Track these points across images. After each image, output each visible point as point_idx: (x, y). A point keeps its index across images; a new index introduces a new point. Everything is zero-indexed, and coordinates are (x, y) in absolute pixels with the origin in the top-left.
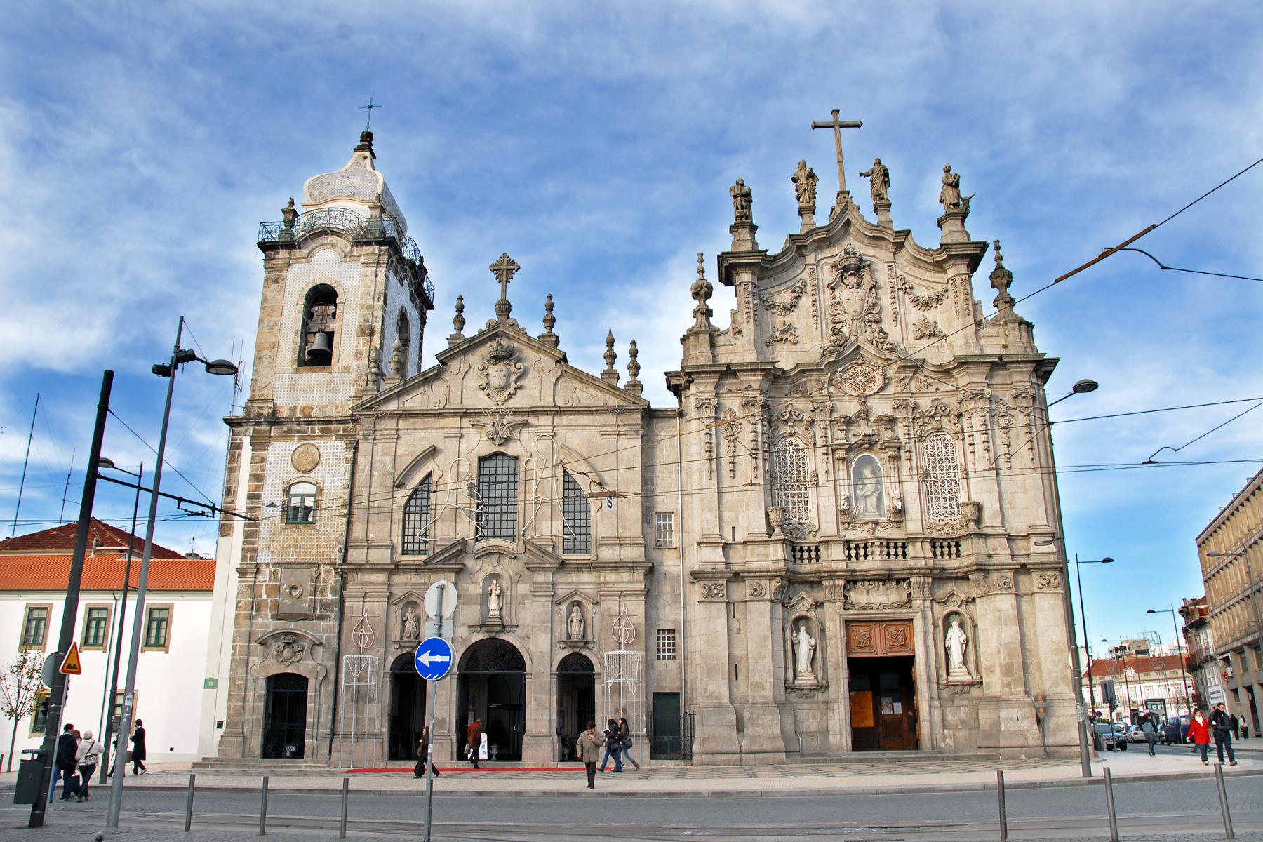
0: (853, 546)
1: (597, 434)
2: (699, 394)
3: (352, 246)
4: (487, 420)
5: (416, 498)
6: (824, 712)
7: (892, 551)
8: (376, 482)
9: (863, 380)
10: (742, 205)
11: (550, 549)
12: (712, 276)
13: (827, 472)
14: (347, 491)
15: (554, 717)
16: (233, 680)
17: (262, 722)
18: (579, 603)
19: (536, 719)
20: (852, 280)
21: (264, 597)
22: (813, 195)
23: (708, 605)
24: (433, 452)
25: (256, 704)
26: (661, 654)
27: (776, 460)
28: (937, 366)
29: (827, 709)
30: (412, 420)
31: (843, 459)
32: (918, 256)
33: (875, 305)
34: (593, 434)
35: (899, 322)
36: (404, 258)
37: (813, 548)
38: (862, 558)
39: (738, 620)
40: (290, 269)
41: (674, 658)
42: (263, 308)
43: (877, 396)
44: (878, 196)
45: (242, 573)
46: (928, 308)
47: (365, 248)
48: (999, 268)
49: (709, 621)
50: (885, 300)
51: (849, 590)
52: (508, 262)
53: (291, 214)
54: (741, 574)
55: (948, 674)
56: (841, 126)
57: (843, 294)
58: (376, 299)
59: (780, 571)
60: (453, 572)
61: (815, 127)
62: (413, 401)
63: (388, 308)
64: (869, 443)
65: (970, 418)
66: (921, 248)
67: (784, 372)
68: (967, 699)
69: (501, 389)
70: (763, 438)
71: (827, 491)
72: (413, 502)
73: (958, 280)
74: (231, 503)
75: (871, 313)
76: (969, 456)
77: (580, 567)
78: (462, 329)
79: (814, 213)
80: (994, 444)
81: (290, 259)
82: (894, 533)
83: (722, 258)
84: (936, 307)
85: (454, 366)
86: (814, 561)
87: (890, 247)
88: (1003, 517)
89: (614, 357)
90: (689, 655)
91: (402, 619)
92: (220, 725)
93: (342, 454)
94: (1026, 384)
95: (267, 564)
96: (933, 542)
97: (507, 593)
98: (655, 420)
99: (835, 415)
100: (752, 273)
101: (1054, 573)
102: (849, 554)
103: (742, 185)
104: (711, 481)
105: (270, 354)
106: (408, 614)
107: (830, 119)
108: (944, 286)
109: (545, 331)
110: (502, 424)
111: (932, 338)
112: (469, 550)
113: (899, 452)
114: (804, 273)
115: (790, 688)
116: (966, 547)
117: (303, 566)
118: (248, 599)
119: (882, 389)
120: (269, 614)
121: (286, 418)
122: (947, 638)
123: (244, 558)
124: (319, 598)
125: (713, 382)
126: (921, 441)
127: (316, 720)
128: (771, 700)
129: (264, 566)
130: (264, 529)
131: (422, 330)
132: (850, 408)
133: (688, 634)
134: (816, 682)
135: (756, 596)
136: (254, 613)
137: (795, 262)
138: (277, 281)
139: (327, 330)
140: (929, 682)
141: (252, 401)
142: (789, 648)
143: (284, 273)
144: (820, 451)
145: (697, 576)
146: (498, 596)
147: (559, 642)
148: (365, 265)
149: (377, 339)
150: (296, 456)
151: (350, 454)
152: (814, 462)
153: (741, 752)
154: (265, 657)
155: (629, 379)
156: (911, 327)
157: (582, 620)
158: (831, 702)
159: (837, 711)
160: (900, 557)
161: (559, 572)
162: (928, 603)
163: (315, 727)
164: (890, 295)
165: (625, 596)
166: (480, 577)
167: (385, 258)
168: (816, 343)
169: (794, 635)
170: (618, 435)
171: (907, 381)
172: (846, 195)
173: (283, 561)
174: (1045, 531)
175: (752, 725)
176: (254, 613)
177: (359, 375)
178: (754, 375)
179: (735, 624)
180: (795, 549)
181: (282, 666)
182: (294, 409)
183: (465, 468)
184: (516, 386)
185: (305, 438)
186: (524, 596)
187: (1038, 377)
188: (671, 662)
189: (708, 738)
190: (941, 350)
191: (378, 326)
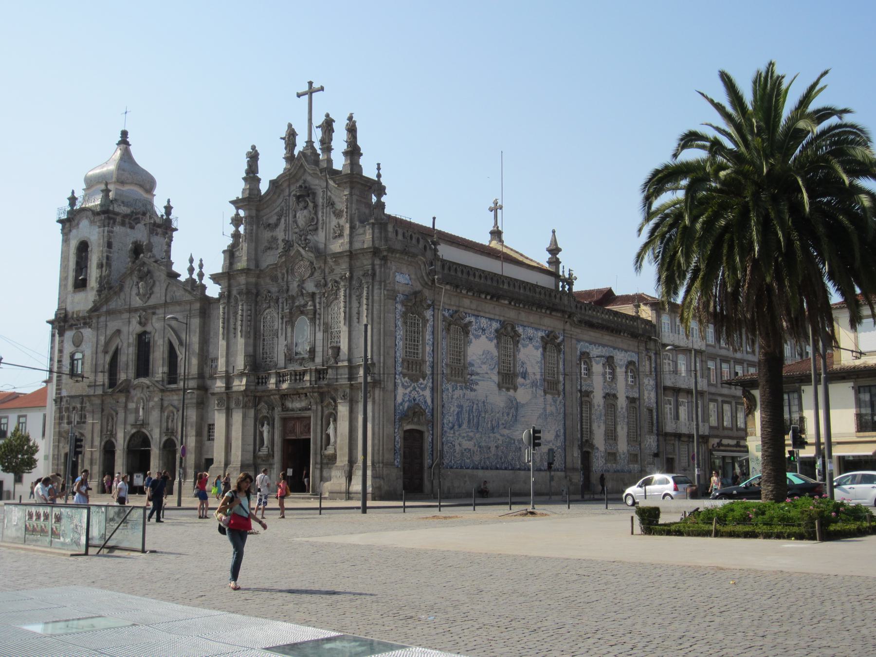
7: (298, 377)
13: (282, 329)
16: (54, 455)
44: (322, 142)
45: (56, 401)
53: (73, 200)
62: (113, 305)
69: (144, 295)
107: (306, 88)
115: (255, 456)
118: (58, 415)
119: (312, 274)
123: (56, 394)
141: (59, 309)
148: (99, 227)
152: (277, 324)
156: (332, 231)
162: (320, 408)
183: (131, 340)
187: (381, 259)
191: (104, 262)
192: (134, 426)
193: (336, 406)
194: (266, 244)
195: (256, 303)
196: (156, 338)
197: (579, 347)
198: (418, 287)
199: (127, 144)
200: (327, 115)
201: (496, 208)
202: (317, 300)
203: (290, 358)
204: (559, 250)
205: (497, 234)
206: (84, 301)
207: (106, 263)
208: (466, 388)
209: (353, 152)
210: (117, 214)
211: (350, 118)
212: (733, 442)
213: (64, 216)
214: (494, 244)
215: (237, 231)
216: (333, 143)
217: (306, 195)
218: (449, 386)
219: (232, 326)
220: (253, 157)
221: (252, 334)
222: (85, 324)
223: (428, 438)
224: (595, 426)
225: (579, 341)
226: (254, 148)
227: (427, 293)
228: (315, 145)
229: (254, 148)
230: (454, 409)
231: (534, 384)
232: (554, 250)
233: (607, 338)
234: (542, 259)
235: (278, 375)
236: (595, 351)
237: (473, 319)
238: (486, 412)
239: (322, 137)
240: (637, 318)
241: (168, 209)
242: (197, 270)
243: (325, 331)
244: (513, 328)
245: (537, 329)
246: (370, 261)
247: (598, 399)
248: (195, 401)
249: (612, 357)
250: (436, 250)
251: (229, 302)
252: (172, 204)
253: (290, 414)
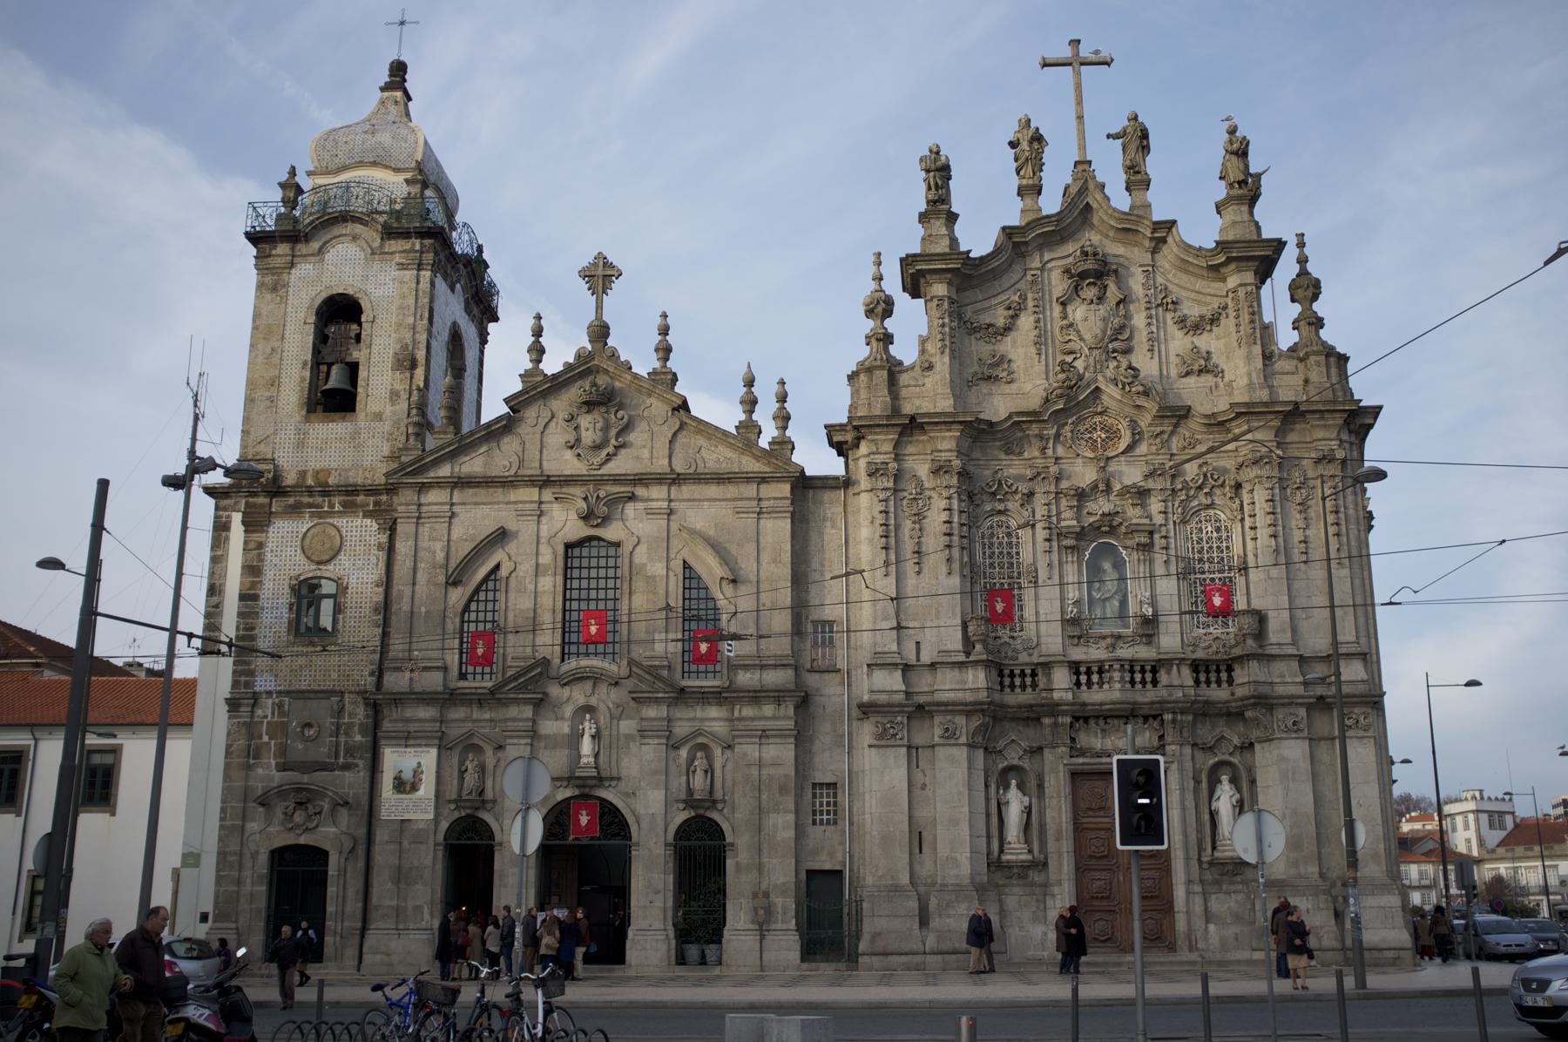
0: (1083, 669)
1: (730, 512)
2: (872, 457)
3: (382, 239)
4: (578, 491)
5: (478, 601)
6: (1041, 898)
7: (1138, 677)
8: (422, 577)
9: (1103, 436)
10: (936, 184)
11: (665, 673)
12: (893, 285)
14: (381, 590)
15: (670, 903)
16: (222, 855)
17: (264, 913)
18: (704, 747)
19: (645, 907)
20: (1090, 293)
21: (266, 738)
22: (1039, 166)
23: (882, 751)
24: (501, 536)
25: (255, 888)
26: (818, 817)
27: (978, 547)
28: (1206, 416)
29: (1045, 895)
30: (471, 491)
31: (1072, 548)
32: (1186, 258)
33: (1122, 327)
34: (723, 512)
35: (1156, 353)
36: (456, 253)
37: (1028, 672)
38: (1096, 686)
39: (923, 771)
40: (293, 271)
41: (835, 823)
42: (255, 328)
43: (1123, 459)
45: (233, 704)
46: (1198, 332)
47: (401, 242)
48: (1303, 273)
49: (882, 773)
50: (1139, 320)
51: (1077, 731)
52: (605, 264)
53: (291, 189)
54: (927, 708)
55: (1214, 848)
56: (1083, 64)
57: (1078, 312)
58: (418, 317)
59: (982, 703)
60: (529, 704)
61: (1045, 65)
62: (473, 464)
63: (434, 330)
65: (1252, 491)
66: (1190, 246)
67: (991, 424)
68: (1241, 883)
69: (597, 447)
70: (960, 517)
71: (1050, 594)
72: (473, 606)
73: (1241, 292)
74: (217, 606)
75: (1117, 339)
76: (1250, 545)
77: (706, 697)
78: (540, 361)
79: (1039, 193)
80: (1284, 528)
81: (293, 256)
82: (1143, 652)
83: (907, 261)
84: (1211, 330)
85: (530, 414)
86: (1029, 690)
87: (1147, 243)
88: (1294, 630)
89: (754, 402)
90: (855, 819)
91: (460, 769)
92: (204, 918)
93: (373, 538)
94: (1334, 443)
95: (269, 693)
96: (1196, 666)
97: (605, 733)
98: (811, 491)
99: (1064, 484)
100: (948, 283)
101: (1363, 710)
102: (1078, 680)
103: (938, 153)
104: (888, 578)
105: (267, 394)
106: (468, 763)
107: (1066, 52)
108: (1222, 300)
109: (657, 365)
110: (598, 496)
111: (1203, 375)
112: (553, 673)
113: (1151, 538)
114: (1023, 281)
115: (996, 865)
116: (1240, 675)
117: (320, 695)
118: (241, 743)
119: (1130, 448)
120: (273, 762)
121: (294, 486)
122: (1216, 797)
123: (235, 684)
124: (342, 739)
125: (892, 439)
126: (1184, 522)
127: (340, 908)
128: (967, 881)
129: (264, 696)
131: (482, 352)
132: (1084, 475)
133: (855, 789)
134: (1029, 857)
135: (947, 738)
136: (252, 762)
137: (1010, 265)
138: (274, 289)
139: (349, 359)
140: (1187, 859)
142: (994, 810)
143: (285, 276)
144: (1041, 534)
145: (866, 710)
146: (593, 737)
147: (677, 801)
148: (402, 267)
149: (420, 372)
150: (307, 541)
151: (384, 538)
153: (925, 953)
154: (268, 821)
155: (775, 433)
156: (1173, 359)
157: (709, 771)
158: (1051, 885)
159: (1059, 897)
160: (1149, 686)
161: (676, 705)
163: (339, 920)
164: (1144, 314)
165: (768, 737)
166: (568, 711)
167: (429, 257)
168: (1038, 382)
169: (1001, 792)
170: (759, 513)
171: (1166, 436)
172: (1086, 167)
173: (293, 688)
174: (1353, 650)
175: (940, 916)
176: (252, 762)
177: (396, 424)
178: (949, 430)
179: (918, 776)
180: (1002, 672)
181: (292, 835)
182: (303, 474)
183: (546, 558)
184: (616, 444)
185: (320, 515)
186: (629, 737)
187: (1350, 432)
188: (831, 828)
189: (879, 934)
190: (1215, 393)
191: (421, 355)
194: (976, 368)
195: (971, 496)
196: (641, 556)
219: (908, 546)
220: (939, 172)
248: (791, 724)
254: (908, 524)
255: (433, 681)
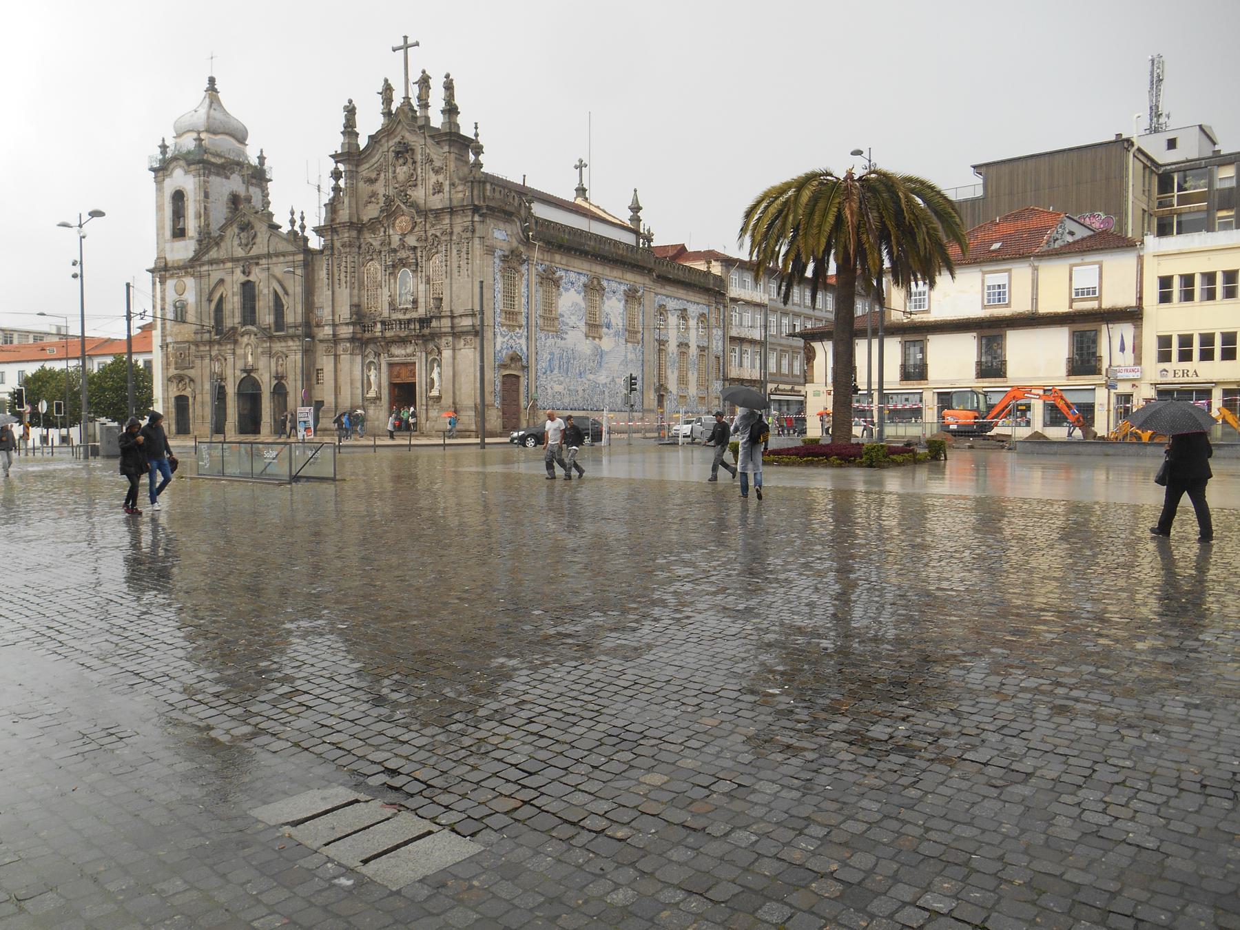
44: (419, 98)
45: (161, 347)
53: (164, 148)
61: (394, 50)
62: (213, 254)
64: (403, 263)
77: (280, 338)
82: (414, 315)
107: (402, 44)
115: (364, 399)
130: (168, 324)
148: (194, 176)
162: (424, 354)
167: (202, 171)
183: (235, 290)
185: (179, 277)
187: (480, 216)
192: (244, 371)
193: (440, 353)
196: (261, 288)
197: (657, 299)
198: (515, 244)
199: (216, 91)
200: (424, 72)
201: (580, 166)
202: (419, 254)
203: (393, 306)
204: (641, 208)
205: (581, 191)
206: (183, 250)
207: (204, 213)
208: (557, 337)
209: (451, 110)
210: (213, 164)
211: (447, 76)
212: (788, 387)
213: (156, 165)
214: (579, 201)
215: (337, 183)
216: (429, 100)
217: (404, 151)
218: (542, 335)
219: (336, 277)
220: (351, 111)
221: (356, 285)
222: (187, 273)
223: (523, 382)
224: (669, 371)
225: (657, 294)
226: (350, 102)
227: (522, 249)
228: (412, 101)
229: (350, 102)
230: (546, 356)
231: (617, 334)
232: (636, 208)
233: (681, 293)
234: (625, 216)
235: (383, 323)
236: (671, 304)
237: (563, 273)
238: (574, 359)
239: (420, 94)
240: (708, 273)
241: (262, 159)
242: (298, 223)
243: (428, 282)
244: (599, 283)
245: (620, 283)
246: (470, 219)
247: (672, 347)
249: (685, 310)
250: (530, 208)
251: (332, 254)
252: (264, 154)
253: (396, 360)
254: (335, 268)
255: (206, 336)
